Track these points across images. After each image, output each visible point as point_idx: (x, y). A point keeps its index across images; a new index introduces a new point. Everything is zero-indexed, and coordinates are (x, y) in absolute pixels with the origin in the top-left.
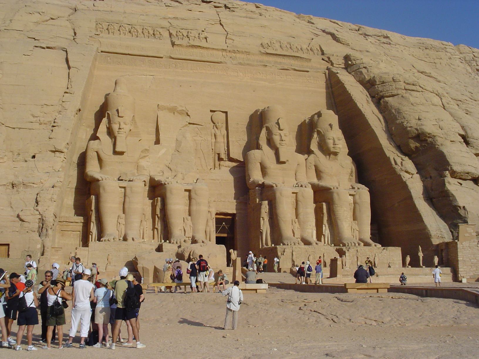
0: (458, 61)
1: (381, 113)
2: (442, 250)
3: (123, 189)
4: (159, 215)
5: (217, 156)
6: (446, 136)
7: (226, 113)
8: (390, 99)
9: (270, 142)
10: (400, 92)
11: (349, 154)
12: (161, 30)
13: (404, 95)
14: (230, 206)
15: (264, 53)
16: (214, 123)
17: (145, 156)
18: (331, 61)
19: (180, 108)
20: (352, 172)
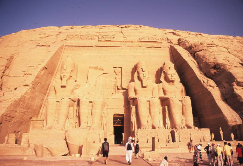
0: (236, 43)
1: (196, 60)
2: (236, 130)
3: (58, 103)
4: (78, 116)
5: (117, 87)
6: (231, 64)
7: (121, 68)
8: (200, 53)
9: (139, 78)
10: (204, 48)
11: (180, 82)
12: (94, 37)
13: (206, 49)
14: (121, 111)
15: (139, 41)
16: (115, 73)
17: (77, 88)
18: (172, 42)
19: (100, 67)
20: (182, 91)
